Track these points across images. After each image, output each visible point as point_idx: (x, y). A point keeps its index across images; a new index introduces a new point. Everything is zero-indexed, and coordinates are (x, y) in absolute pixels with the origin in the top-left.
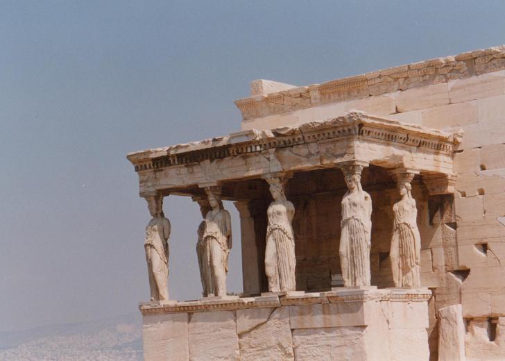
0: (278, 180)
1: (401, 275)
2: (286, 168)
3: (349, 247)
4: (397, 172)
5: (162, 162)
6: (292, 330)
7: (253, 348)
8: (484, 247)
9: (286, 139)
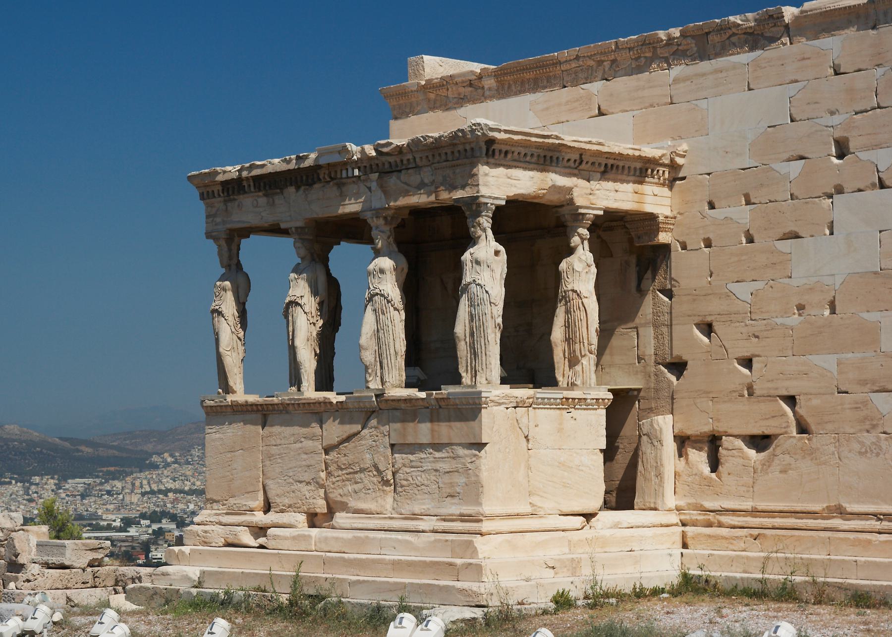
0: (381, 222)
1: (567, 368)
3: (467, 325)
4: (565, 211)
5: (234, 187)
6: (392, 446)
7: (342, 469)
8: (708, 329)
9: (391, 159)
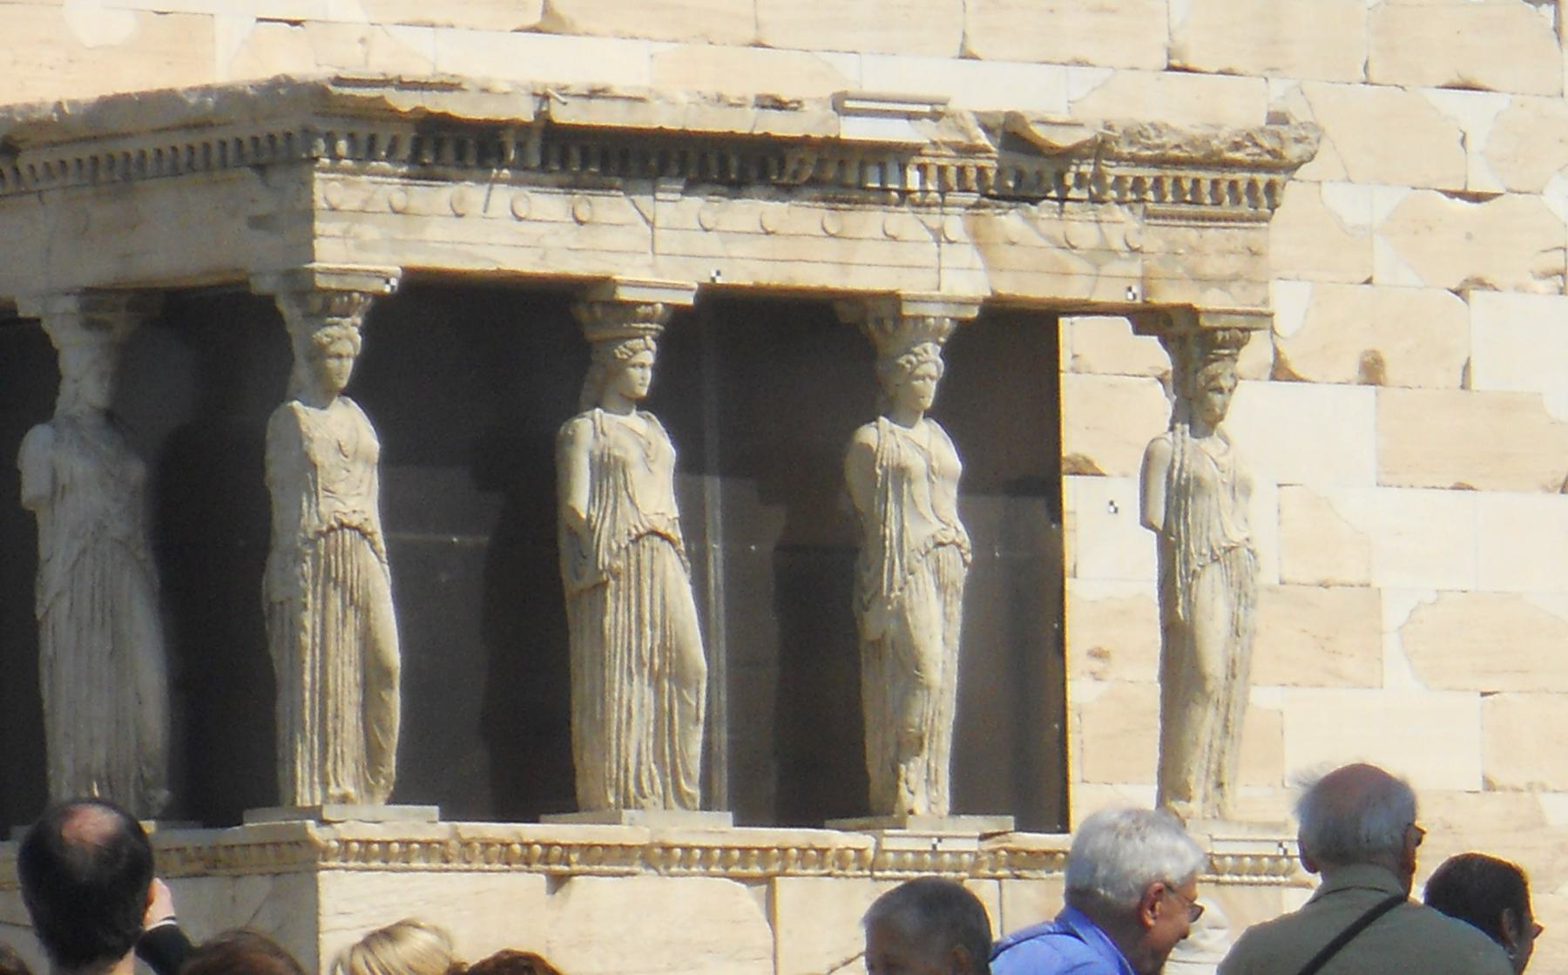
2: (1008, 287)
